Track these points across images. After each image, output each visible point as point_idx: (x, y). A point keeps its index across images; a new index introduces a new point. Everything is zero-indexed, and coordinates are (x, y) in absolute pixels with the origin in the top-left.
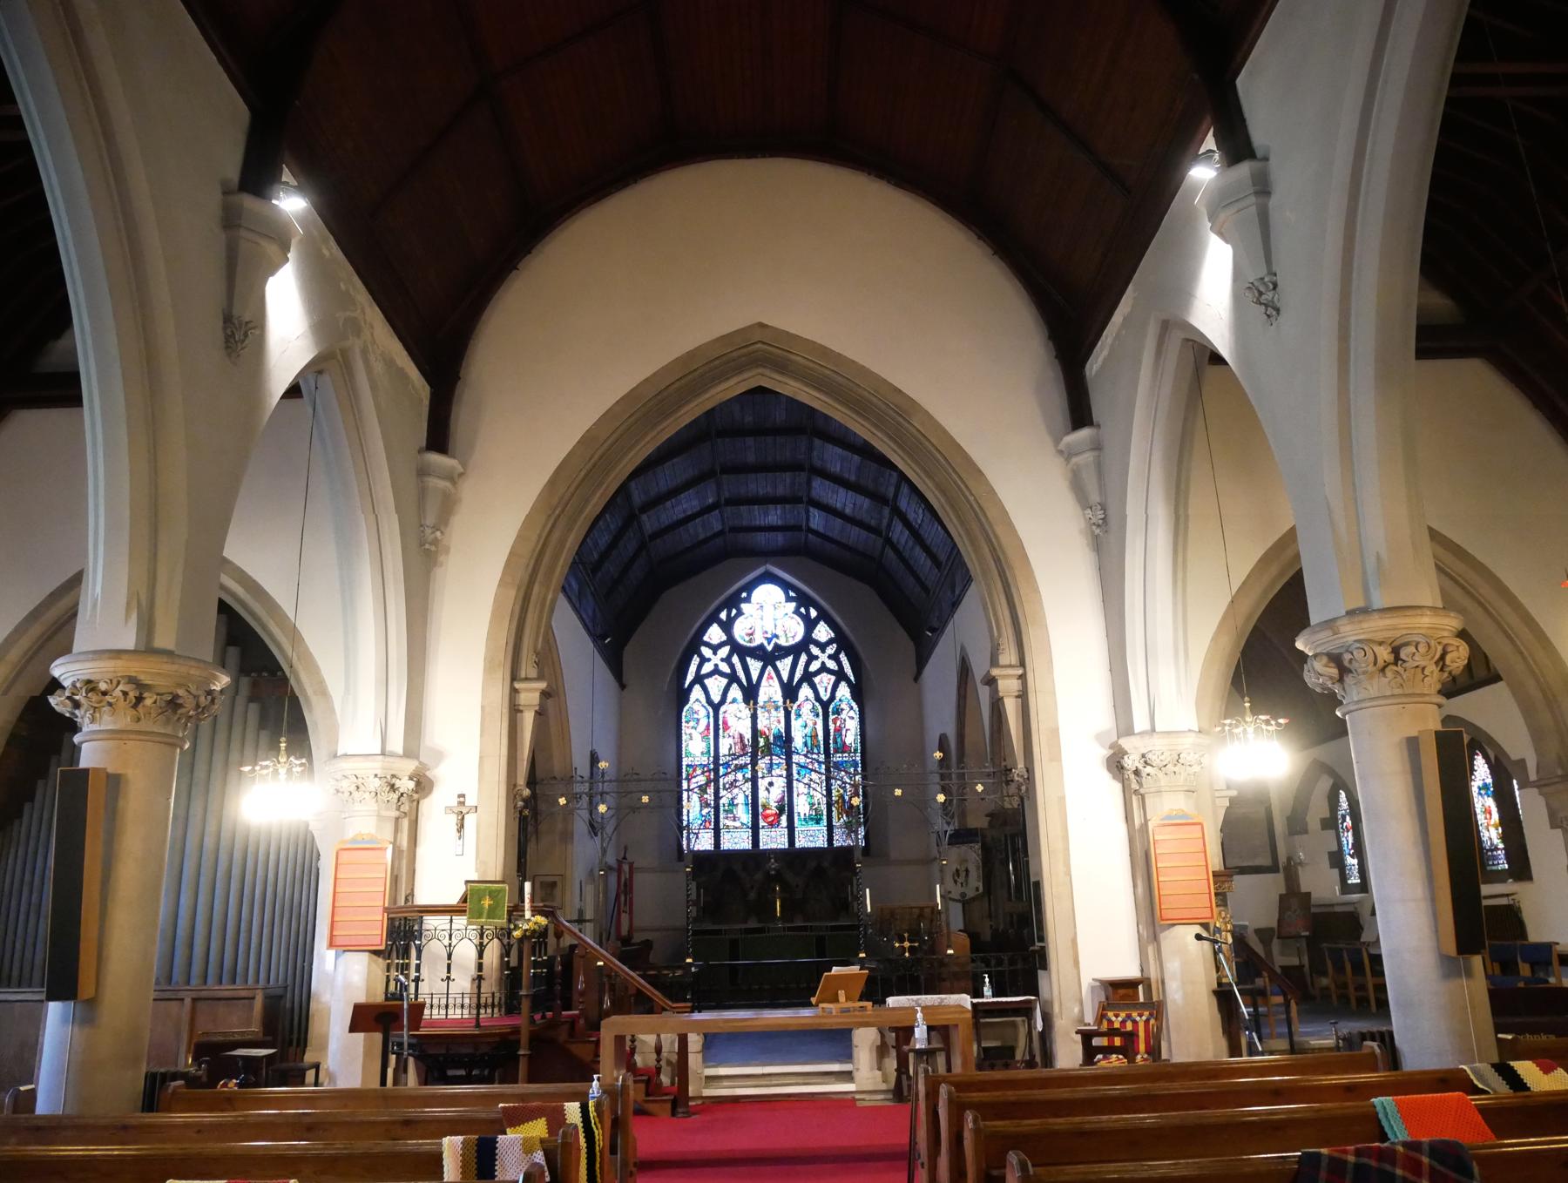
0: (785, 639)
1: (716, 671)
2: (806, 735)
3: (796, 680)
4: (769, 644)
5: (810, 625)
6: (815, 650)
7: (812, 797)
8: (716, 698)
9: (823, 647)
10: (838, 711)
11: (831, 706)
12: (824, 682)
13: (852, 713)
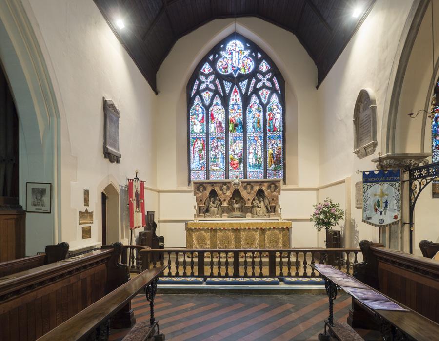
0: (244, 71)
1: (207, 89)
2: (254, 122)
3: (249, 92)
4: (235, 73)
5: (258, 62)
6: (260, 76)
7: (256, 154)
8: (207, 103)
9: (264, 74)
10: (271, 110)
11: (268, 107)
12: (264, 93)
13: (279, 110)
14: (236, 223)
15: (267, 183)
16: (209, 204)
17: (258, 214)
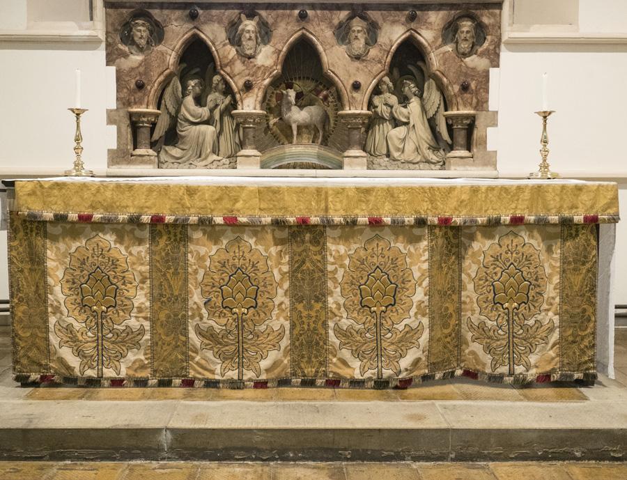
14: (302, 191)
15: (442, 14)
16: (179, 104)
17: (396, 154)
